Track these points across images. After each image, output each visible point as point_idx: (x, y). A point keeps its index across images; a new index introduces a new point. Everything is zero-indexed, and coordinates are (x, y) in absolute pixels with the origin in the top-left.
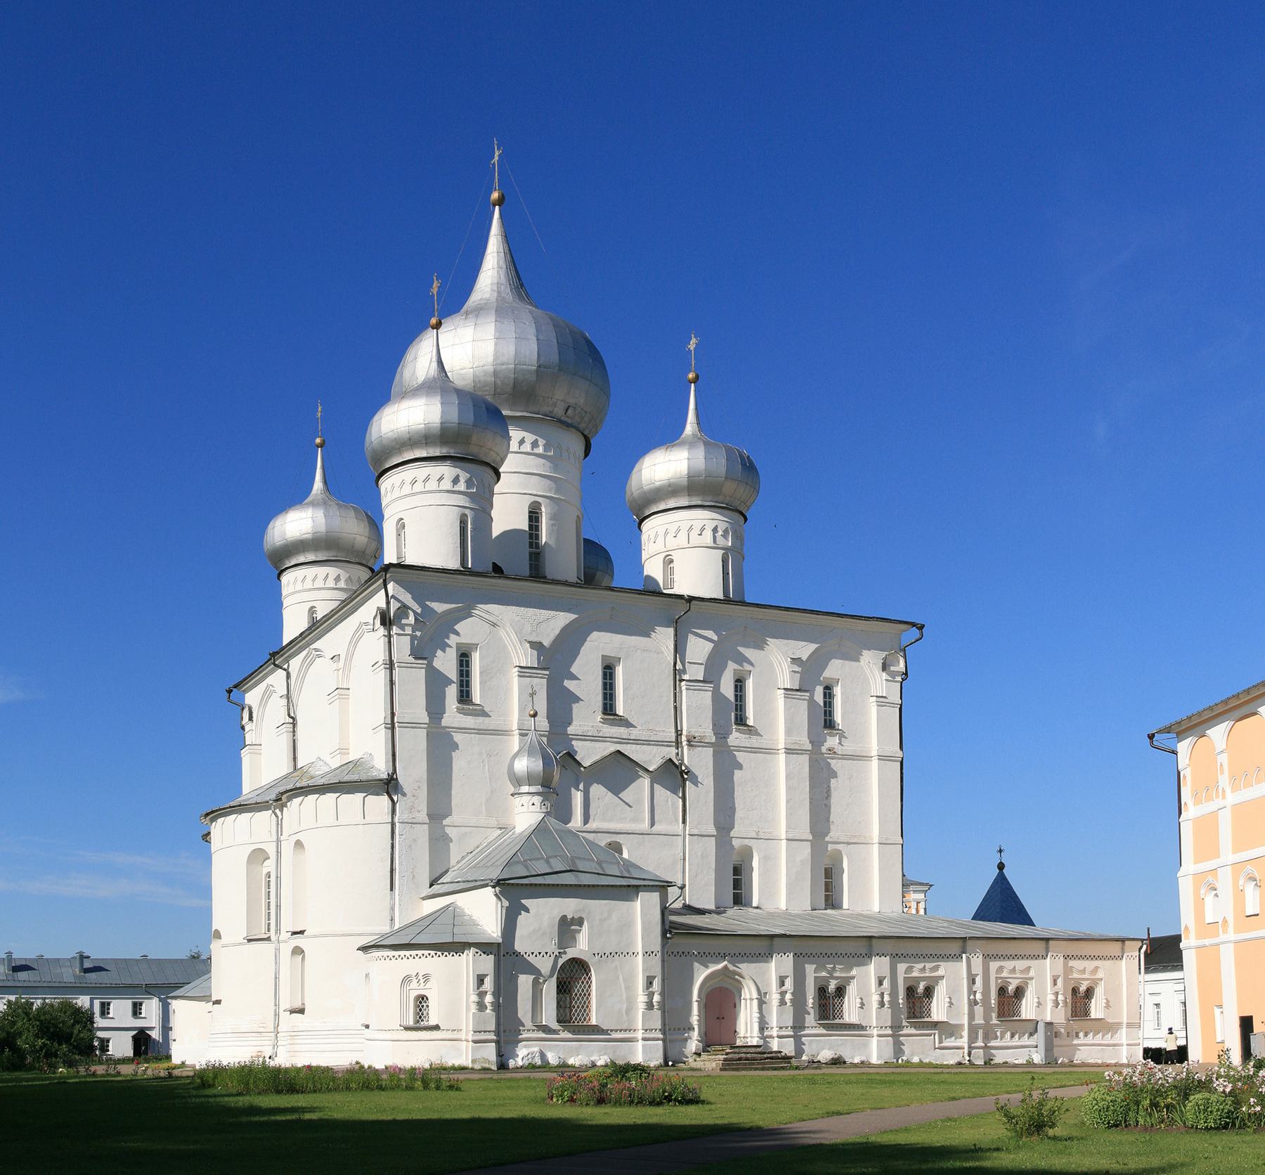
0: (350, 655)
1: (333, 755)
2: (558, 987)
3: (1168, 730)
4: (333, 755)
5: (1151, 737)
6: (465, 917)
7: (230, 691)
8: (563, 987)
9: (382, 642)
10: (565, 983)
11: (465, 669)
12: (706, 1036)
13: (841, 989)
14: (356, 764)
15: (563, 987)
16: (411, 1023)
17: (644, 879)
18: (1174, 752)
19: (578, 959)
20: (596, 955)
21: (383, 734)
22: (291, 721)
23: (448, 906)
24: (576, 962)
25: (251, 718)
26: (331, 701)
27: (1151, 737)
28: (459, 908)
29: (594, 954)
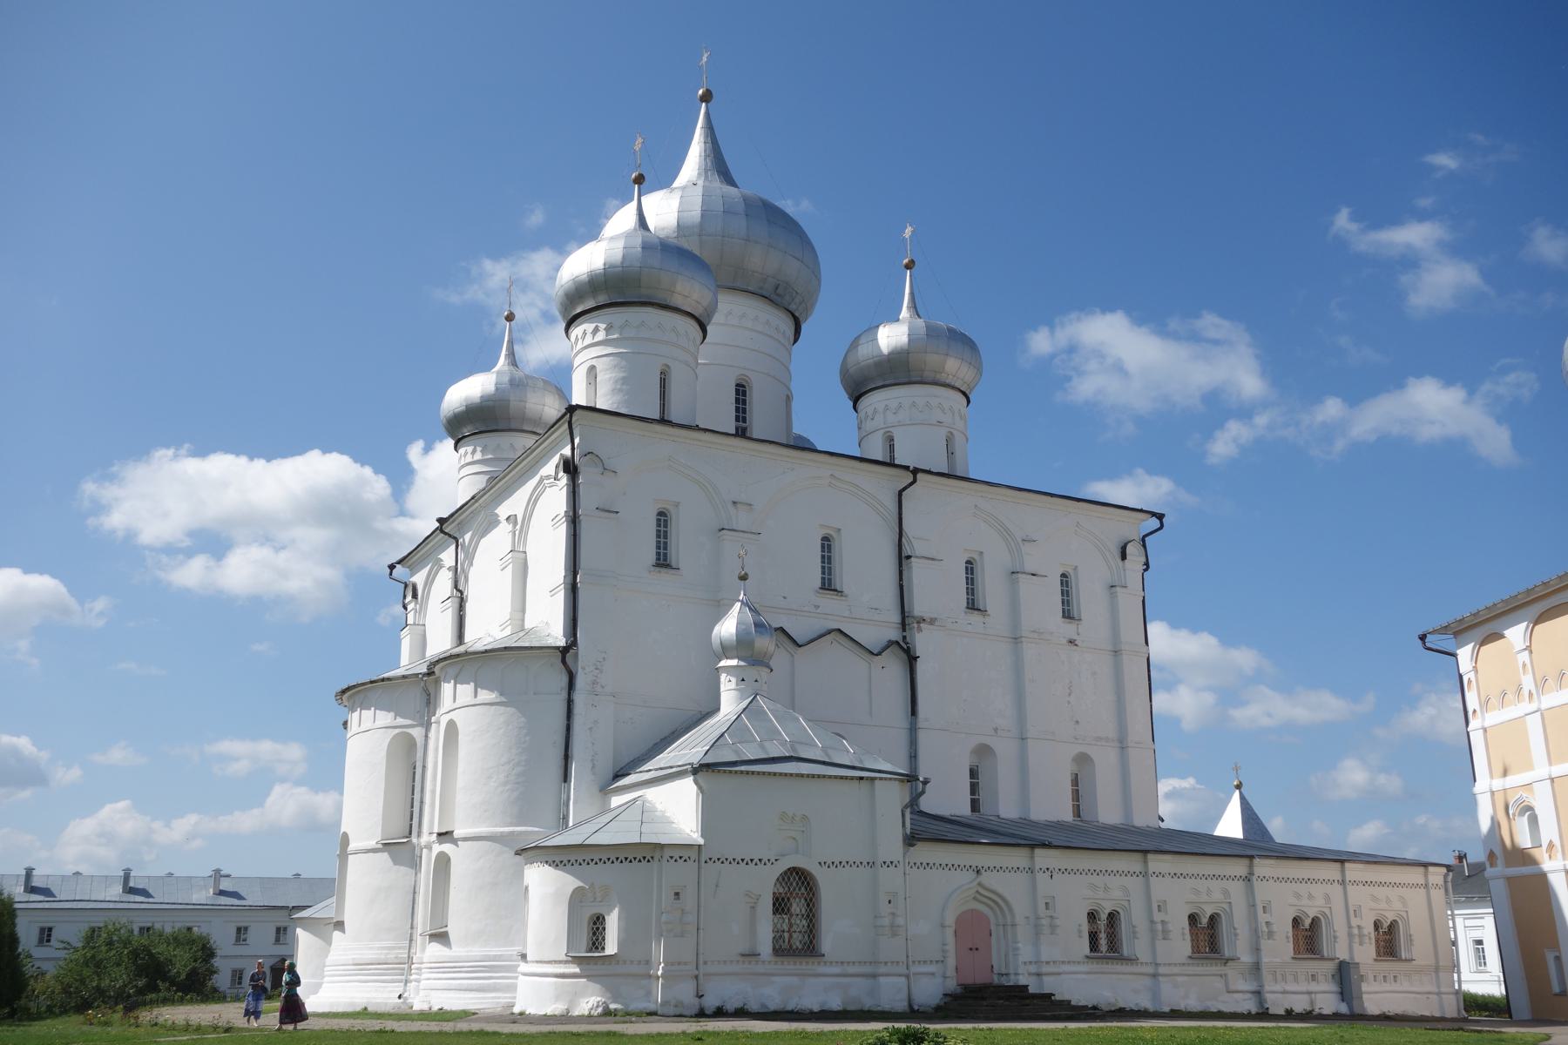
1: (502, 627)
2: (774, 905)
3: (1444, 630)
4: (502, 627)
5: (1423, 638)
6: (657, 814)
7: (392, 567)
8: (780, 904)
10: (783, 899)
12: (957, 972)
13: (1114, 915)
15: (780, 904)
18: (1454, 655)
19: (800, 869)
20: (823, 864)
23: (635, 800)
24: (797, 873)
25: (415, 596)
26: (504, 566)
27: (1423, 638)
28: (649, 802)
29: (820, 863)
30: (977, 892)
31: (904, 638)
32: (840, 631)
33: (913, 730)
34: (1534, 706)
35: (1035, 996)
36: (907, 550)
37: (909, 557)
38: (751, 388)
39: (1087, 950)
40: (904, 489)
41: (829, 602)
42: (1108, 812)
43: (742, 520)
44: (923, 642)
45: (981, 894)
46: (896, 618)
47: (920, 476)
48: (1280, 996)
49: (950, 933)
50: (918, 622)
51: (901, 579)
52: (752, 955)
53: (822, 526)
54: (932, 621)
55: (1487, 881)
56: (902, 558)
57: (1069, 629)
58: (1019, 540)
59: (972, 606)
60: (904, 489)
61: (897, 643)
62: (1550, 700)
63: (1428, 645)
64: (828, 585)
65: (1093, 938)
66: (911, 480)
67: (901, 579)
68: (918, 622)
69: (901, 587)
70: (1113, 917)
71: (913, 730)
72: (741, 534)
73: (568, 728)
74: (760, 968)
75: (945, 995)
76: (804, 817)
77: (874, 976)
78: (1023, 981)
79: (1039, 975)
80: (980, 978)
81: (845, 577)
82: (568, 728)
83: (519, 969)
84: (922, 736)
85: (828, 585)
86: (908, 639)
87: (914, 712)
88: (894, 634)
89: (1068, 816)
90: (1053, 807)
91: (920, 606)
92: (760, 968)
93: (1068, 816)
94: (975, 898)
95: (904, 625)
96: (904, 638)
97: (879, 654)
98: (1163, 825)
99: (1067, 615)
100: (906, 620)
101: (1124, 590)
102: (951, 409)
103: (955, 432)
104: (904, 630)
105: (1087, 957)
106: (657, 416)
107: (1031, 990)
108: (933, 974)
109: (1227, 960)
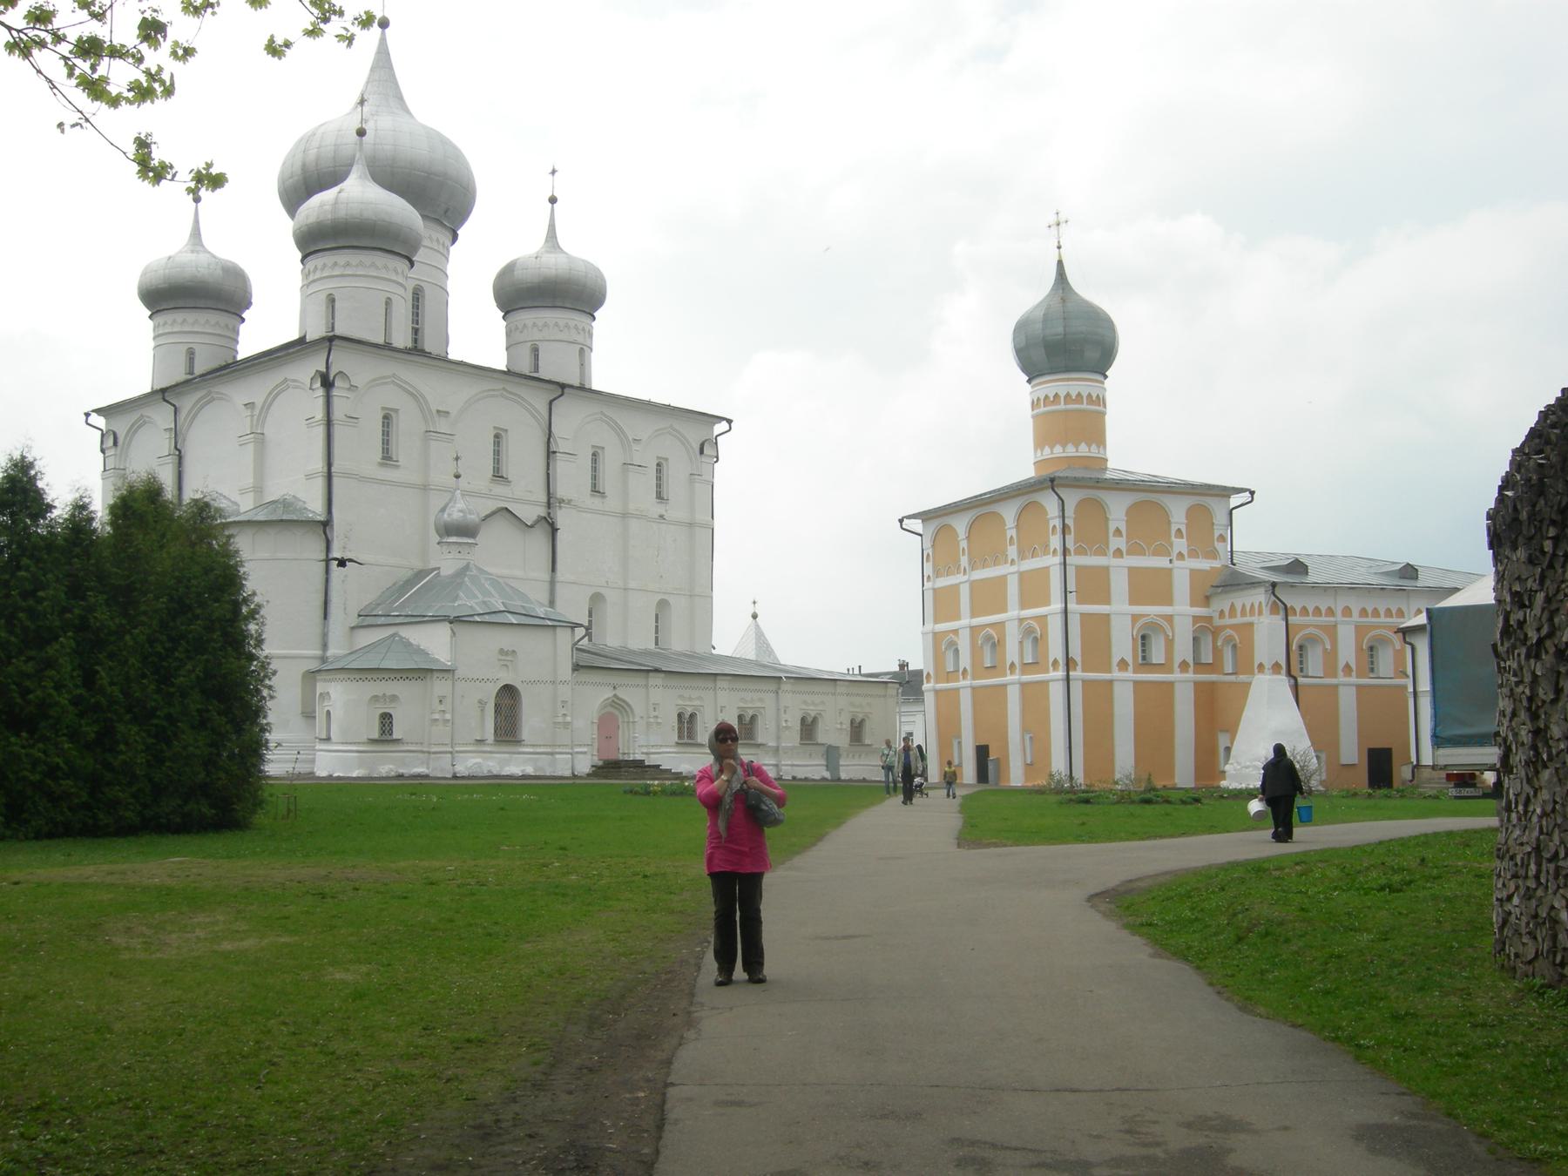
0: (267, 406)
9: (321, 402)
11: (386, 429)
14: (285, 504)
16: (376, 735)
17: (559, 621)
21: (319, 484)
22: (177, 453)
23: (394, 635)
25: (115, 443)
30: (613, 701)
31: (549, 514)
32: (506, 509)
33: (552, 583)
34: (966, 578)
35: (649, 766)
36: (553, 448)
37: (555, 452)
38: (423, 297)
39: (676, 738)
40: (555, 399)
41: (499, 489)
42: (677, 642)
43: (443, 426)
44: (562, 518)
45: (615, 703)
46: (544, 499)
47: (566, 390)
48: (789, 768)
49: (595, 727)
50: (560, 503)
51: (548, 469)
52: (481, 742)
53: (495, 428)
54: (569, 502)
55: (922, 693)
56: (550, 454)
57: (660, 509)
58: (631, 439)
59: (596, 490)
60: (555, 399)
61: (545, 518)
62: (979, 575)
63: (904, 526)
64: (498, 476)
65: (680, 729)
66: (560, 393)
67: (548, 469)
68: (560, 503)
69: (548, 474)
70: (693, 716)
71: (552, 583)
72: (443, 436)
73: (327, 581)
74: (488, 749)
75: (593, 766)
76: (514, 651)
77: (552, 754)
78: (638, 757)
79: (647, 754)
80: (612, 756)
81: (510, 471)
82: (327, 581)
83: (317, 748)
84: (559, 588)
85: (498, 476)
86: (551, 515)
87: (554, 569)
88: (542, 512)
89: (652, 646)
90: (640, 640)
91: (561, 491)
92: (488, 749)
93: (652, 646)
94: (612, 706)
95: (549, 505)
96: (549, 514)
97: (532, 526)
98: (714, 652)
99: (659, 496)
100: (551, 501)
101: (699, 477)
102: (584, 329)
103: (585, 347)
104: (549, 508)
105: (677, 743)
106: (381, 341)
107: (647, 764)
108: (585, 753)
109: (759, 746)
